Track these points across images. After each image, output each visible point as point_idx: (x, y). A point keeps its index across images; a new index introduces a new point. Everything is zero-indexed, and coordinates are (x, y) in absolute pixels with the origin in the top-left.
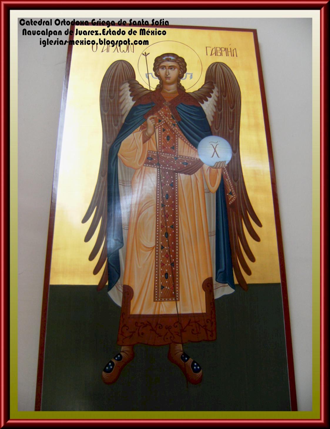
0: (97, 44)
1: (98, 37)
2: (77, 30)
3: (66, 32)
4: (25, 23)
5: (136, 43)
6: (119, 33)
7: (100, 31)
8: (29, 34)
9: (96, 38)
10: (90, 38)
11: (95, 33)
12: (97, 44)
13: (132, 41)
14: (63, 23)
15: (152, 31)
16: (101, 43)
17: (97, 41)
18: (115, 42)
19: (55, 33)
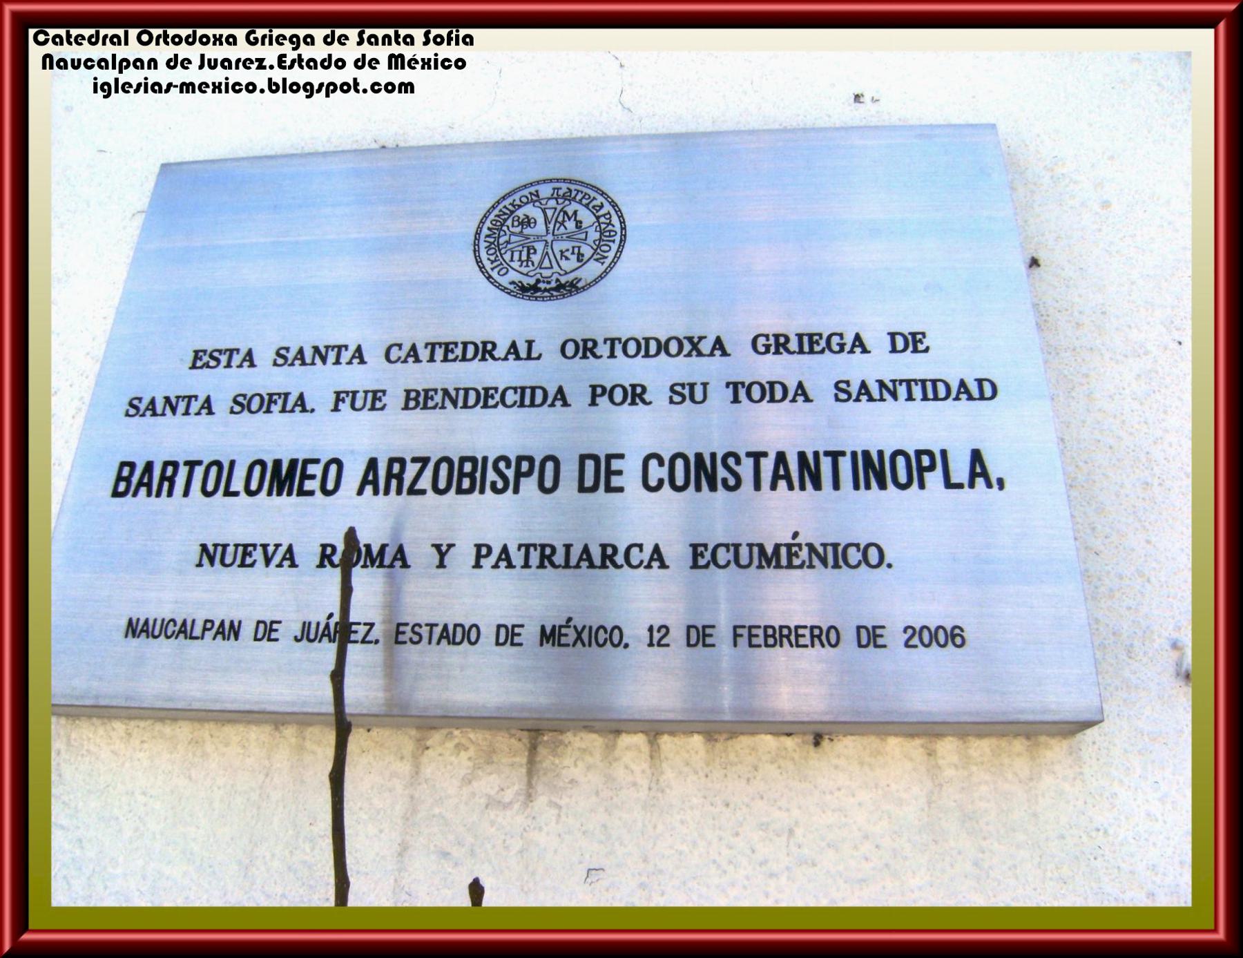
0: (262, 91)
1: (267, 73)
2: (202, 56)
3: (170, 61)
4: (50, 41)
5: (376, 88)
6: (326, 63)
7: (271, 59)
8: (60, 67)
9: (260, 78)
10: (240, 76)
11: (256, 64)
12: (262, 91)
13: (365, 83)
14: (161, 40)
15: (423, 60)
16: (274, 88)
17: (262, 83)
18: (316, 87)
19: (138, 64)
